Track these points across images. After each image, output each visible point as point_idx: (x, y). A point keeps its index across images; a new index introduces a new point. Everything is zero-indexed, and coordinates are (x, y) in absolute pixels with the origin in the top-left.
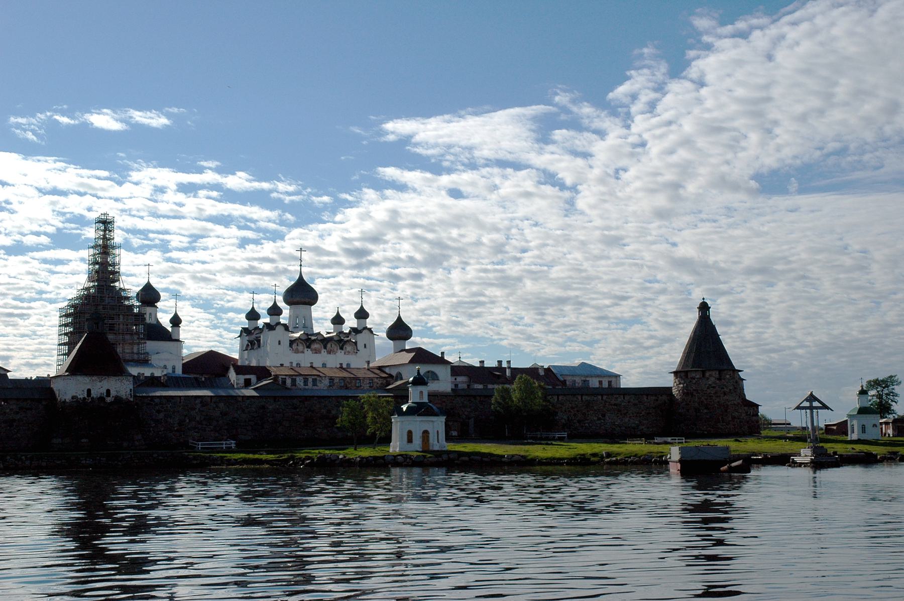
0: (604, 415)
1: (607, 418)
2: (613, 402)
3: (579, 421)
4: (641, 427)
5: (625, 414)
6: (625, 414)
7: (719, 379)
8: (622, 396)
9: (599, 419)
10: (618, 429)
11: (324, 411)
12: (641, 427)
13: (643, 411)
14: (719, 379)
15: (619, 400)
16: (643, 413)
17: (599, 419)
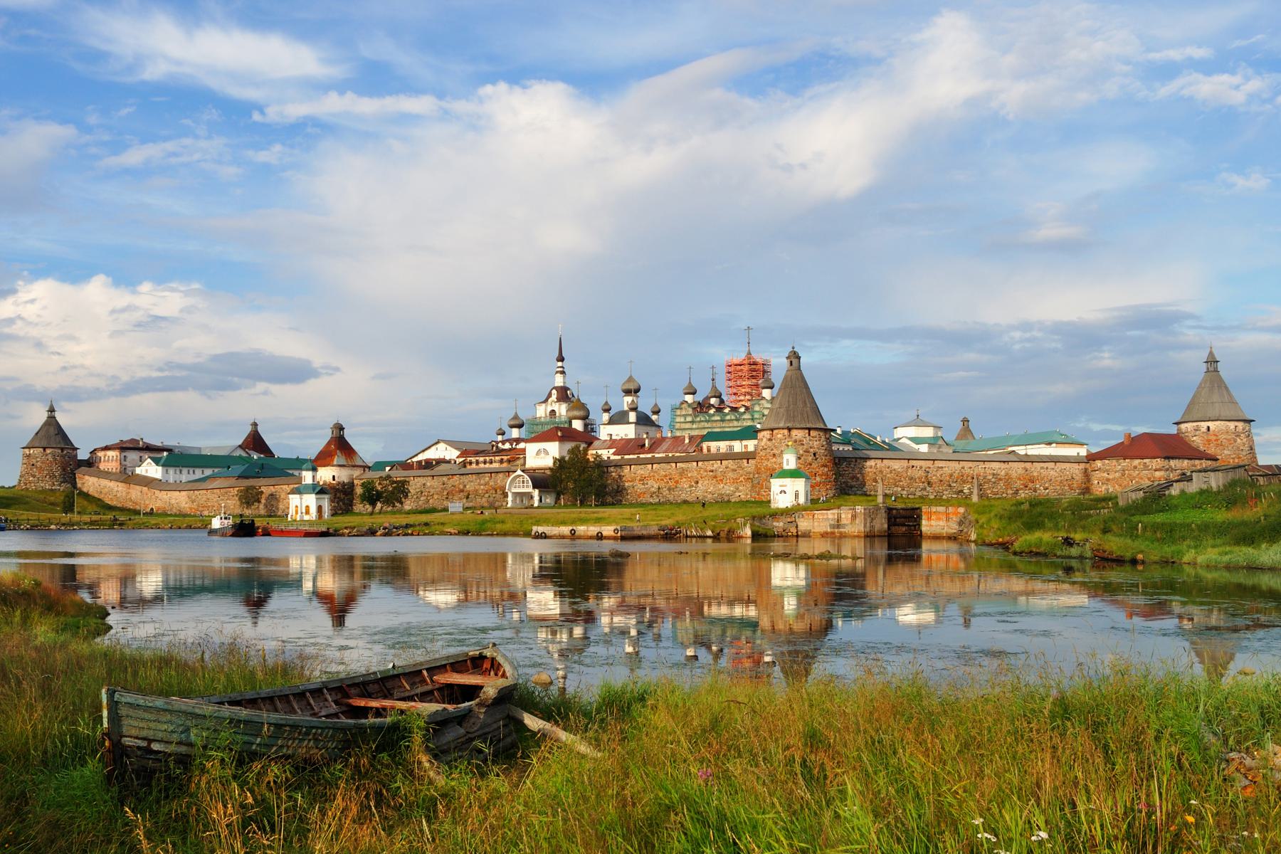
0: (697, 482)
1: (699, 485)
2: (709, 468)
3: (669, 489)
4: (737, 494)
5: (721, 480)
6: (721, 480)
7: (770, 440)
8: (719, 462)
9: (692, 486)
10: (710, 496)
11: (461, 487)
12: (737, 494)
13: (742, 476)
14: (770, 440)
15: (715, 466)
16: (741, 479)
17: (691, 486)
